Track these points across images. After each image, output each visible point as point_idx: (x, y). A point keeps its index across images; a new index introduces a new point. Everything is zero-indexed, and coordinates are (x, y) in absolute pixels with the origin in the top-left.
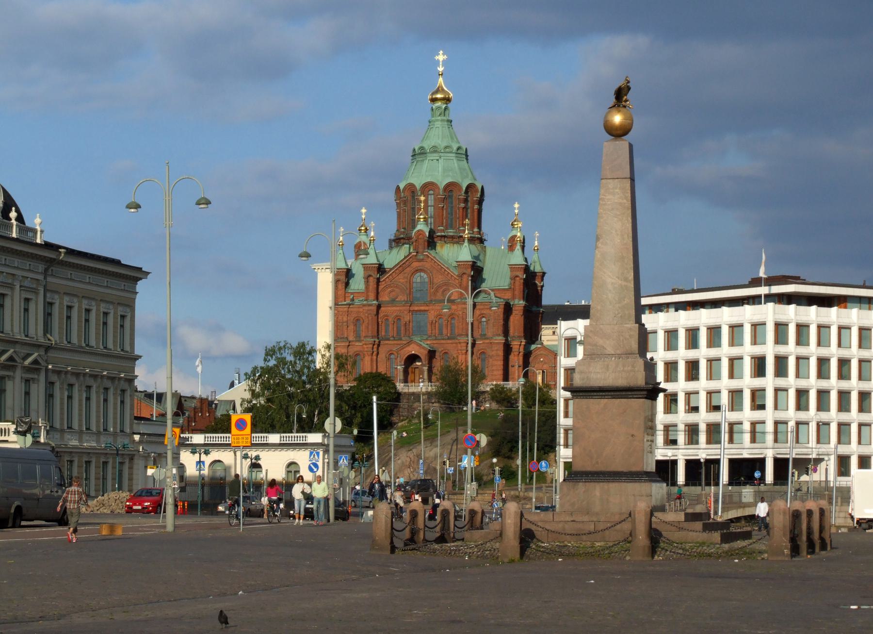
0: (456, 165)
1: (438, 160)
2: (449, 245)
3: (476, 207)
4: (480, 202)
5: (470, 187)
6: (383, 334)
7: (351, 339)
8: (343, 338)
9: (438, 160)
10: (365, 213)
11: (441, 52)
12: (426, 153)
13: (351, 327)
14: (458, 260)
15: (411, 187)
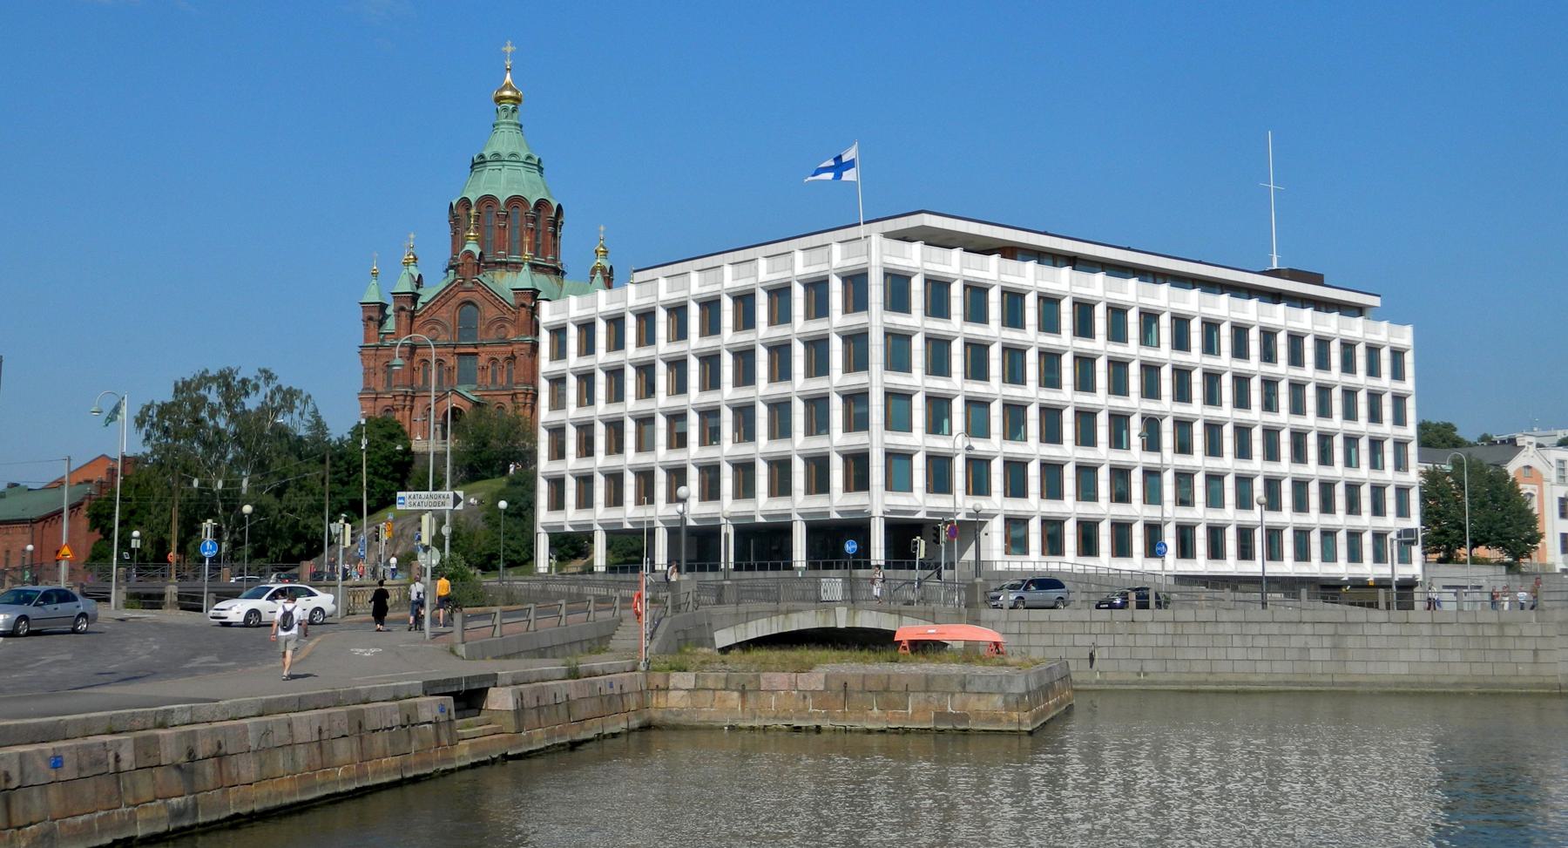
0: (524, 176)
1: (500, 170)
2: (511, 274)
3: (550, 228)
4: (556, 223)
5: (542, 204)
6: (421, 383)
7: (379, 389)
8: (369, 389)
9: (500, 170)
10: (414, 240)
11: (509, 42)
12: (485, 162)
13: (380, 375)
14: (515, 287)
15: (465, 202)
